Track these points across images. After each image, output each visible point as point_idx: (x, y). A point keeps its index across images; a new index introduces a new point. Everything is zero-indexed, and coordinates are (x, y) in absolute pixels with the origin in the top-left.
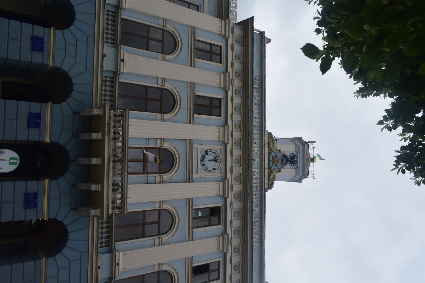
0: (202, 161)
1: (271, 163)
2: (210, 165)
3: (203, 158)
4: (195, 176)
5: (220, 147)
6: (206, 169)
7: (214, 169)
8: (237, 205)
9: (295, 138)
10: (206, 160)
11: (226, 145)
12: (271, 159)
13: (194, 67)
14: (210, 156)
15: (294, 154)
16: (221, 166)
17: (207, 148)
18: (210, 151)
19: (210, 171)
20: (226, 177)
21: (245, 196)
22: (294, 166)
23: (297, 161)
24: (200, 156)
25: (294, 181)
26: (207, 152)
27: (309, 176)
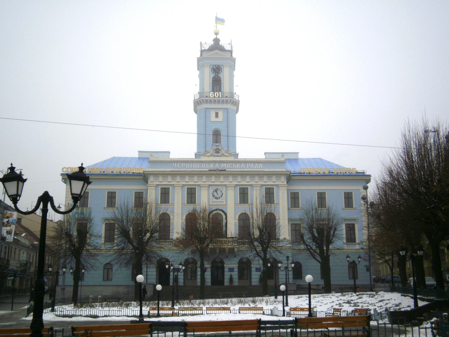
0: (217, 199)
1: (219, 154)
2: (220, 194)
3: (217, 198)
4: (224, 203)
5: (211, 188)
6: (221, 196)
7: (221, 192)
8: (239, 179)
9: (198, 65)
10: (217, 196)
11: (210, 185)
12: (216, 154)
13: (174, 204)
14: (215, 194)
15: (212, 69)
16: (220, 188)
17: (211, 196)
18: (213, 194)
19: (222, 194)
20: (226, 185)
21: (235, 175)
22: (221, 69)
23: (218, 66)
24: (215, 200)
25: (234, 66)
26: (213, 196)
27: (230, 49)
